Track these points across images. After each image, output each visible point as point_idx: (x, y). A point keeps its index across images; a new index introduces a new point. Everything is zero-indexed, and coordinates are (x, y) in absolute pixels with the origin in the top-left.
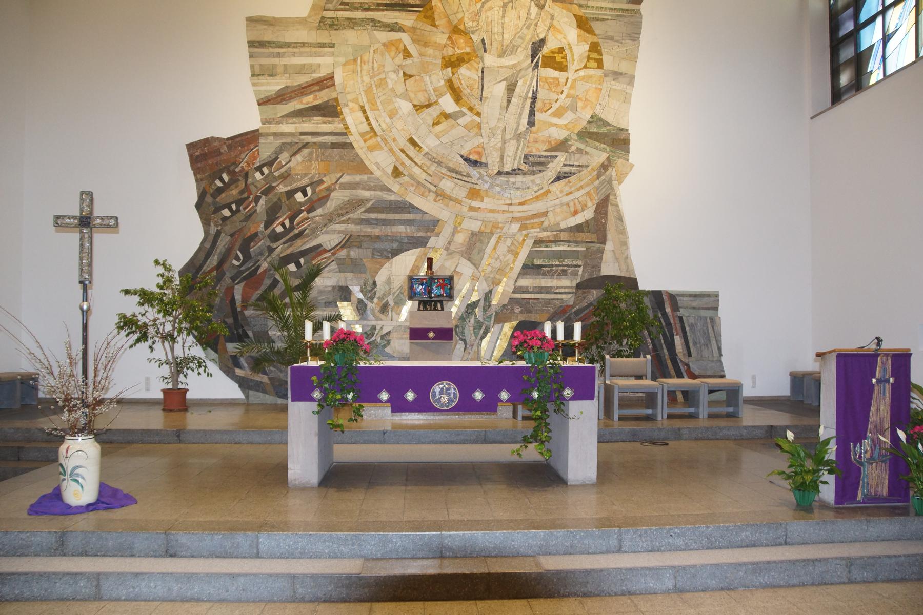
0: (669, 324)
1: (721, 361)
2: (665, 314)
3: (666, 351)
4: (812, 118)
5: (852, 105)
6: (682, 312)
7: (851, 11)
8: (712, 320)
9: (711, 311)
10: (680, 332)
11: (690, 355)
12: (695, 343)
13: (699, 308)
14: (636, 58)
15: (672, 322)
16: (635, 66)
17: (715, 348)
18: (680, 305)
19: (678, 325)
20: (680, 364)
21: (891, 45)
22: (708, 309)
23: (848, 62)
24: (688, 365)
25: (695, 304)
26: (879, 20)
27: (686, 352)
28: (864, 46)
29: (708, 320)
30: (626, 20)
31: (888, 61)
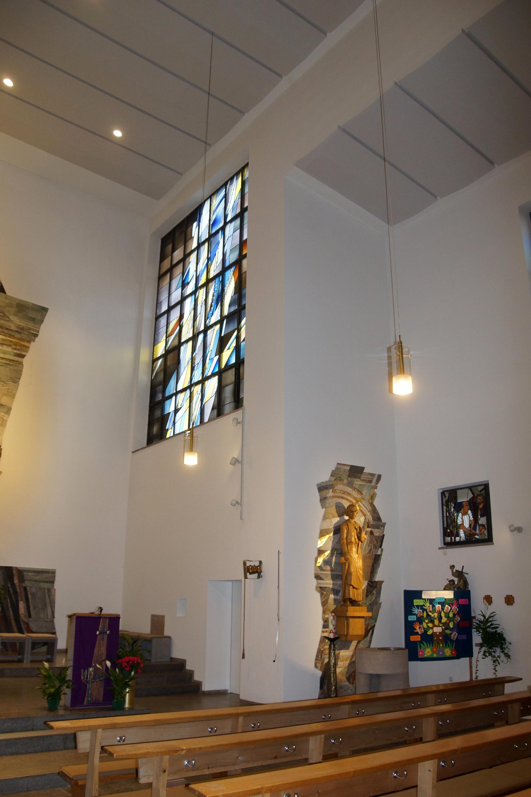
0: (15, 592)
1: (53, 622)
2: (13, 585)
3: (11, 613)
4: (133, 452)
5: (158, 447)
6: (27, 584)
7: (161, 387)
8: (49, 590)
9: (49, 584)
10: (24, 598)
11: (30, 616)
12: (35, 608)
13: (40, 582)
14: (15, 395)
15: (18, 590)
16: (13, 401)
17: (49, 612)
18: (25, 578)
19: (23, 593)
20: (22, 623)
21: (179, 415)
22: (47, 582)
23: (158, 419)
24: (27, 624)
25: (37, 578)
26: (174, 398)
27: (27, 614)
28: (166, 412)
29: (46, 591)
30: (11, 367)
31: (176, 425)
